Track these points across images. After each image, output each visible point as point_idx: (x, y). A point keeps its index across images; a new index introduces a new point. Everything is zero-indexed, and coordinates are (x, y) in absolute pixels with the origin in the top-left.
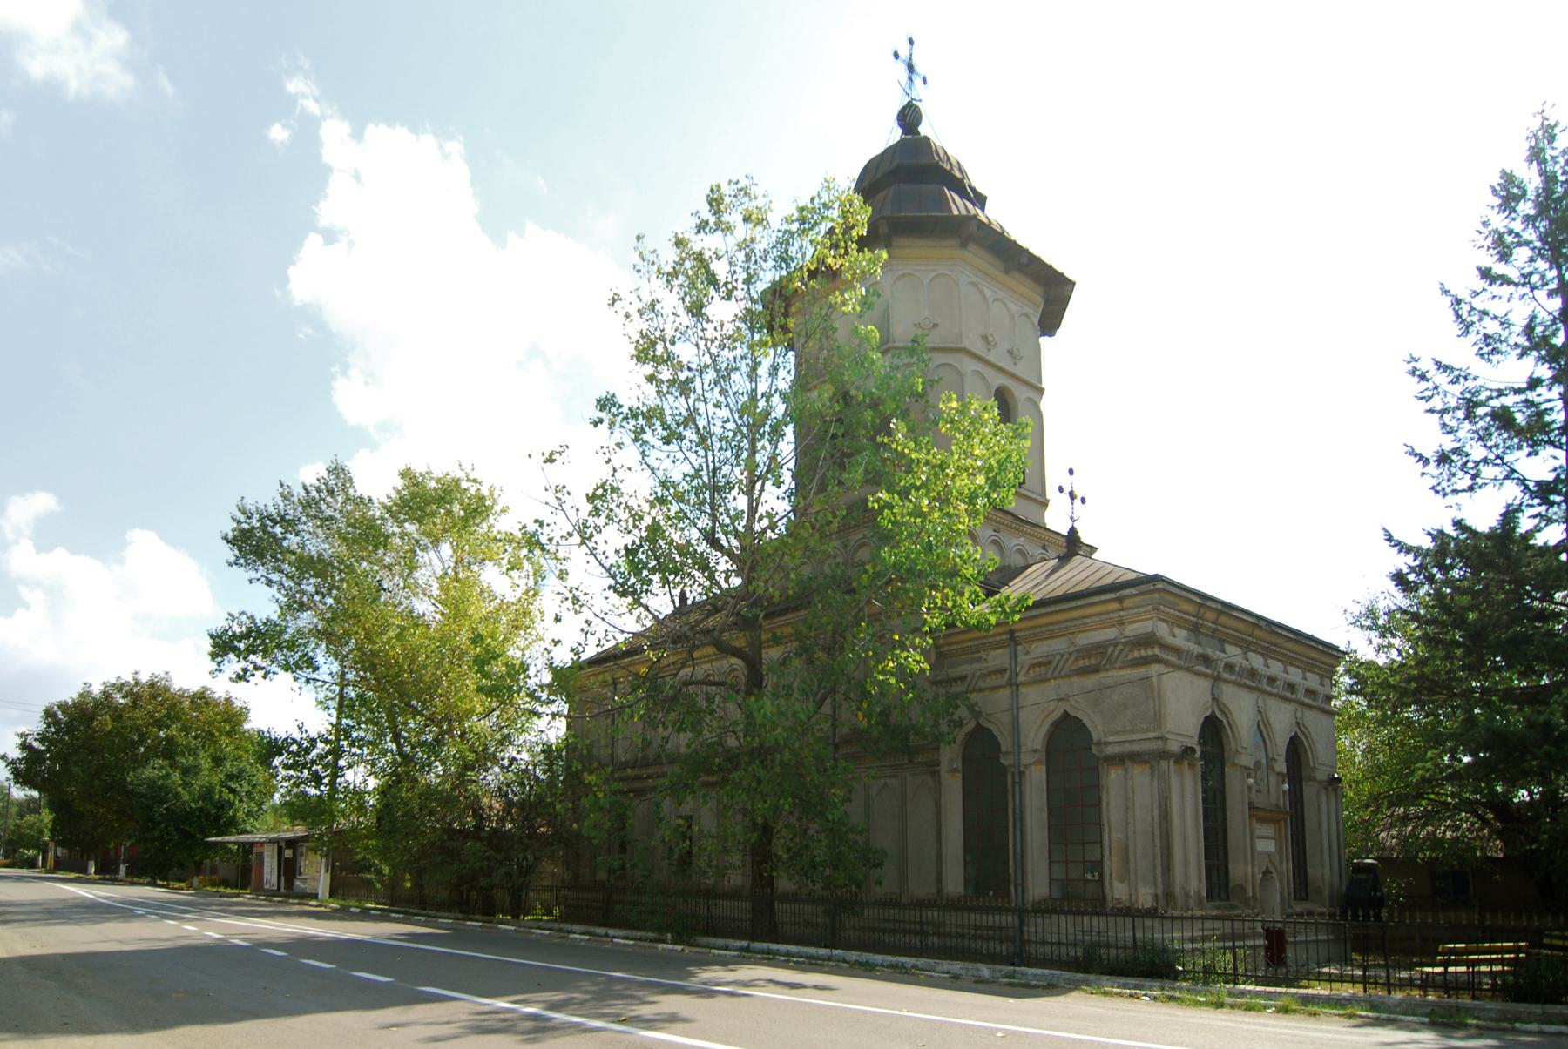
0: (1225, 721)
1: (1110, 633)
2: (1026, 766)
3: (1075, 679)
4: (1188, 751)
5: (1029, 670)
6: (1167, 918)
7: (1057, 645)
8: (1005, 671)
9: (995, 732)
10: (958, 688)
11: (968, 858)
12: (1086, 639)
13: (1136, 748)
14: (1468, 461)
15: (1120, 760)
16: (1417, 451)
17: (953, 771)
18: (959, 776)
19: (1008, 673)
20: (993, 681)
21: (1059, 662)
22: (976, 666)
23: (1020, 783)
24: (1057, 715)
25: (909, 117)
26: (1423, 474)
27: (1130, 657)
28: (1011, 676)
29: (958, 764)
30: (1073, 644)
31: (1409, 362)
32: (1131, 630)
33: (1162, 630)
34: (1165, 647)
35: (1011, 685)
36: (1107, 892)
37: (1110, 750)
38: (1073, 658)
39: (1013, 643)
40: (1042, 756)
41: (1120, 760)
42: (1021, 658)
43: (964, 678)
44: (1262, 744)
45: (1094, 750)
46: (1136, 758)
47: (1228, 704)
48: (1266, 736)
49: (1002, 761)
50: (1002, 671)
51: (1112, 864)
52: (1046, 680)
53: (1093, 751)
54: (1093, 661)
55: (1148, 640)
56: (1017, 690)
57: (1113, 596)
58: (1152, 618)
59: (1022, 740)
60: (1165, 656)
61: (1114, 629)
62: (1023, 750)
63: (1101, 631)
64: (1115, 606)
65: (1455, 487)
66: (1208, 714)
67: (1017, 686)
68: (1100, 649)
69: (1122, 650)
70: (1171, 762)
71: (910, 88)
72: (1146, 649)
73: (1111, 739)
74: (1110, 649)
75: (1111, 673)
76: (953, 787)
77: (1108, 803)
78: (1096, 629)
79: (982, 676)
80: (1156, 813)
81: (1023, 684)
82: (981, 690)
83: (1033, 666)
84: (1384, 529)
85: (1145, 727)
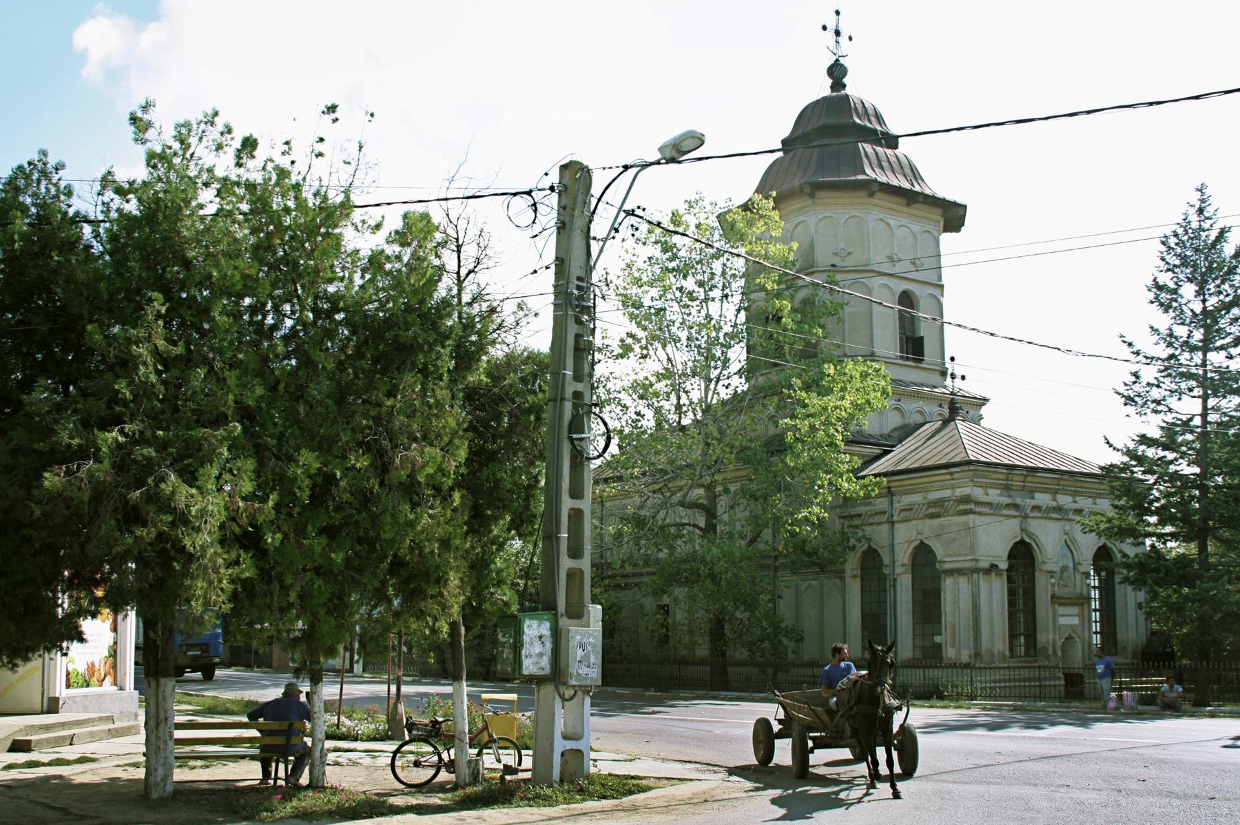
0: (1033, 544)
1: (946, 493)
2: (898, 575)
3: (927, 520)
4: (994, 567)
6: (976, 668)
7: (917, 498)
8: (885, 512)
10: (856, 522)
11: (865, 634)
12: (934, 496)
13: (960, 565)
15: (951, 572)
17: (855, 576)
18: (859, 580)
19: (887, 515)
20: (878, 518)
22: (868, 508)
23: (894, 586)
24: (916, 543)
30: (925, 498)
32: (959, 492)
33: (978, 493)
34: (978, 503)
36: (944, 653)
37: (946, 566)
41: (951, 572)
42: (896, 505)
43: (860, 515)
44: (1069, 555)
45: (937, 566)
47: (1037, 533)
48: (1072, 548)
50: (884, 512)
52: (909, 520)
54: (937, 510)
55: (966, 500)
57: (945, 471)
59: (896, 558)
62: (897, 564)
64: (949, 477)
66: (1018, 539)
67: (893, 523)
68: (939, 503)
70: (981, 574)
73: (947, 559)
76: (854, 588)
79: (872, 515)
81: (898, 522)
82: (871, 524)
83: (902, 510)
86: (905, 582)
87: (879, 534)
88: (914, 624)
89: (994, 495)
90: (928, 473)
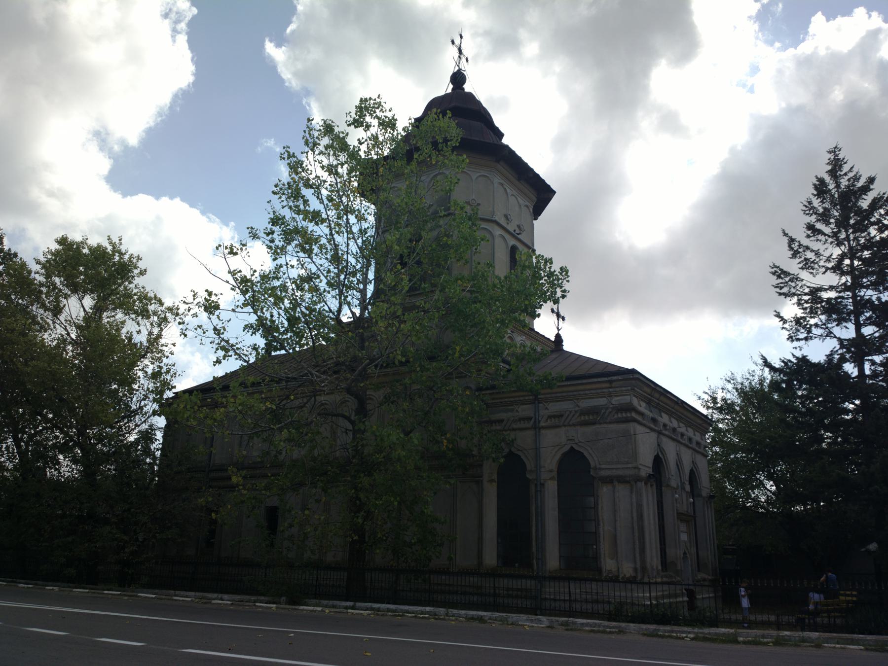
1: (602, 401)
5: (547, 420)
8: (530, 419)
9: (523, 457)
12: (585, 404)
13: (620, 473)
14: (807, 324)
15: (609, 481)
16: (781, 315)
17: (491, 481)
18: (495, 485)
19: (533, 421)
21: (568, 416)
24: (566, 448)
25: (458, 79)
26: (783, 328)
27: (616, 416)
28: (535, 422)
29: (495, 477)
31: (773, 268)
32: (616, 400)
33: (635, 402)
35: (535, 428)
37: (603, 473)
38: (578, 414)
39: (537, 402)
40: (555, 474)
41: (609, 481)
43: (501, 421)
46: (622, 480)
49: (528, 476)
50: (530, 419)
51: (605, 547)
53: (592, 473)
56: (539, 432)
57: (606, 379)
58: (630, 395)
60: (639, 418)
61: (605, 399)
63: (596, 400)
64: (608, 385)
65: (798, 337)
68: (595, 411)
69: (610, 412)
70: (643, 483)
71: (459, 62)
72: (626, 413)
73: (603, 466)
75: (603, 426)
76: (491, 492)
77: (602, 507)
78: (593, 398)
80: (635, 514)
81: (544, 428)
82: (514, 430)
83: (550, 417)
84: (762, 356)
85: (626, 460)
86: (552, 488)
87: (524, 440)
88: (560, 532)
89: (642, 407)
90: (584, 381)
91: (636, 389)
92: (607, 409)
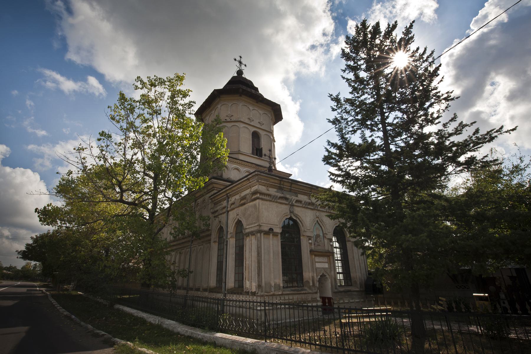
12: (243, 194)
34: (261, 194)
38: (239, 200)
47: (299, 214)
70: (262, 234)
73: (247, 227)
74: (247, 196)
88: (236, 266)
91: (260, 180)
92: (248, 195)
